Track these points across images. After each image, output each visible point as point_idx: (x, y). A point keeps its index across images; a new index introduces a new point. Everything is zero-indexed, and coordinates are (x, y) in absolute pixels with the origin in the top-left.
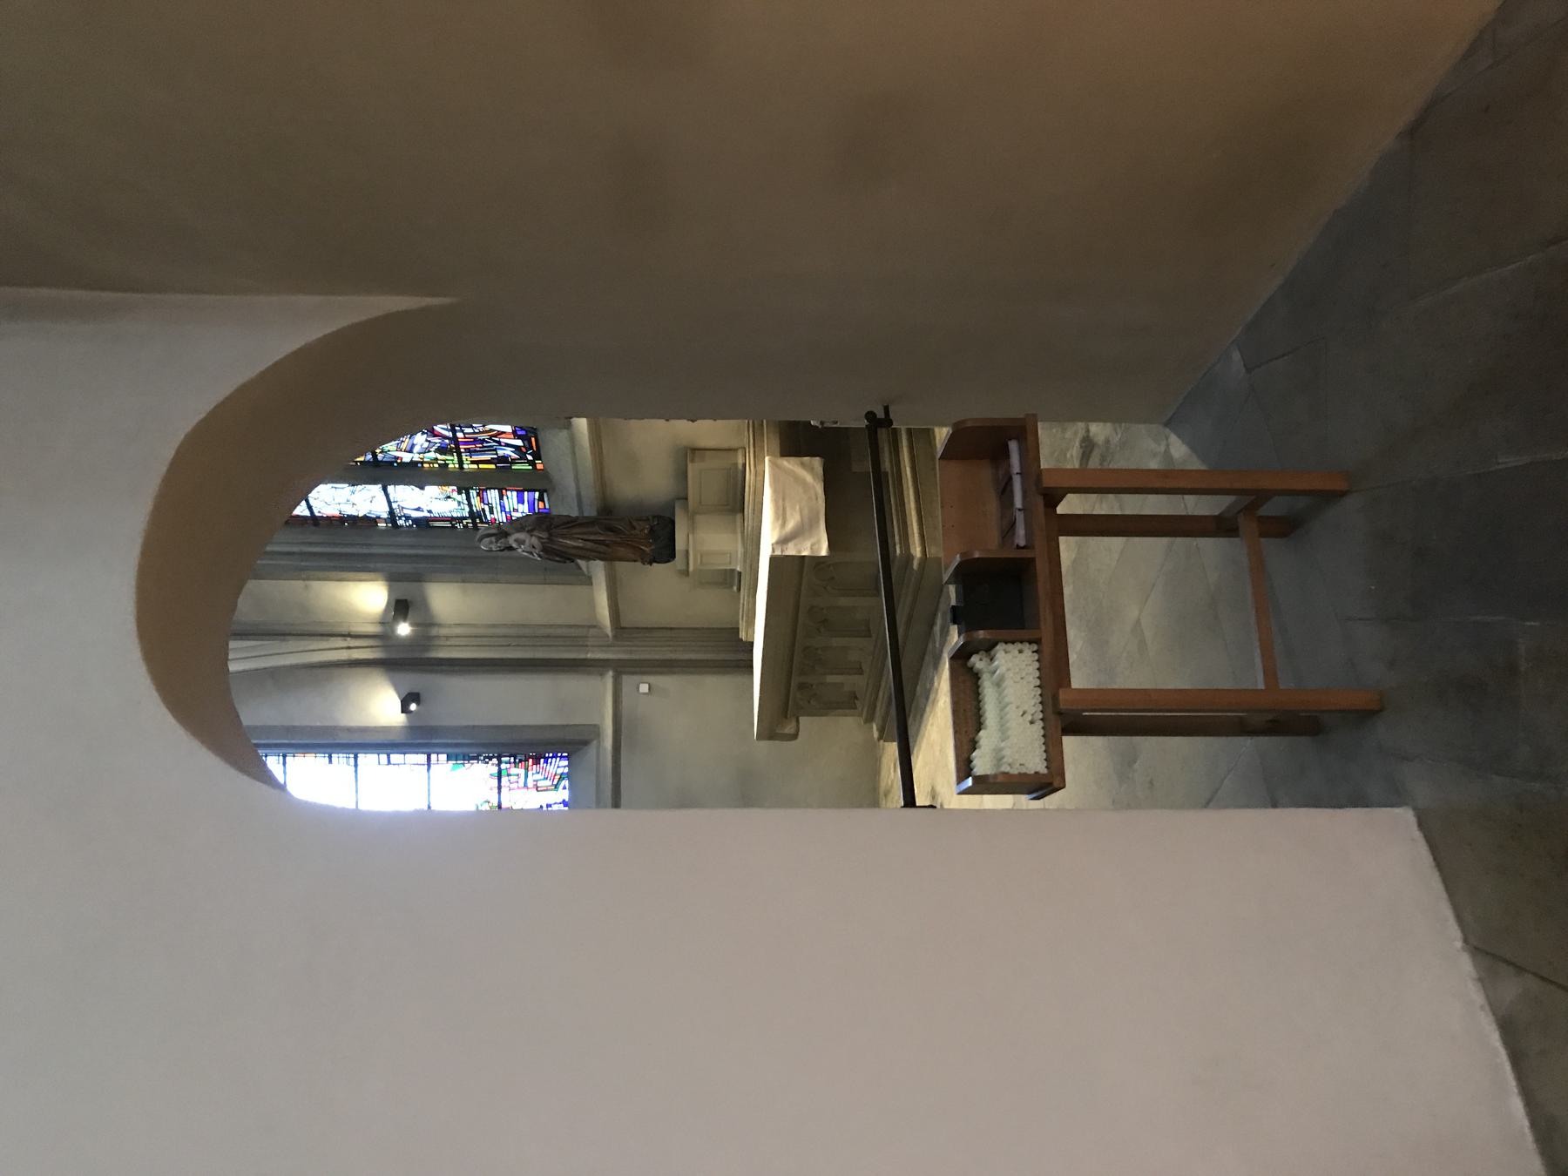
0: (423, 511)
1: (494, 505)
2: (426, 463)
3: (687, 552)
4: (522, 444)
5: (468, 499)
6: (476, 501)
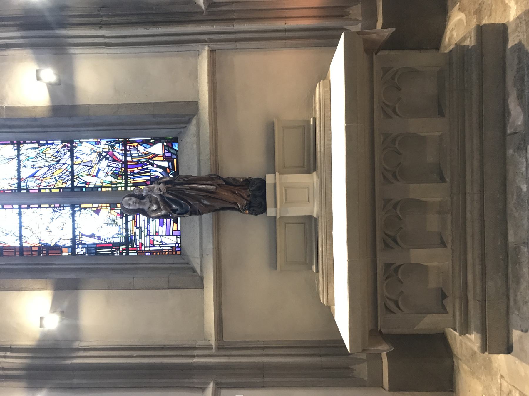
0: (94, 238)
1: (143, 229)
2: (104, 187)
3: (275, 185)
4: (167, 166)
5: (126, 223)
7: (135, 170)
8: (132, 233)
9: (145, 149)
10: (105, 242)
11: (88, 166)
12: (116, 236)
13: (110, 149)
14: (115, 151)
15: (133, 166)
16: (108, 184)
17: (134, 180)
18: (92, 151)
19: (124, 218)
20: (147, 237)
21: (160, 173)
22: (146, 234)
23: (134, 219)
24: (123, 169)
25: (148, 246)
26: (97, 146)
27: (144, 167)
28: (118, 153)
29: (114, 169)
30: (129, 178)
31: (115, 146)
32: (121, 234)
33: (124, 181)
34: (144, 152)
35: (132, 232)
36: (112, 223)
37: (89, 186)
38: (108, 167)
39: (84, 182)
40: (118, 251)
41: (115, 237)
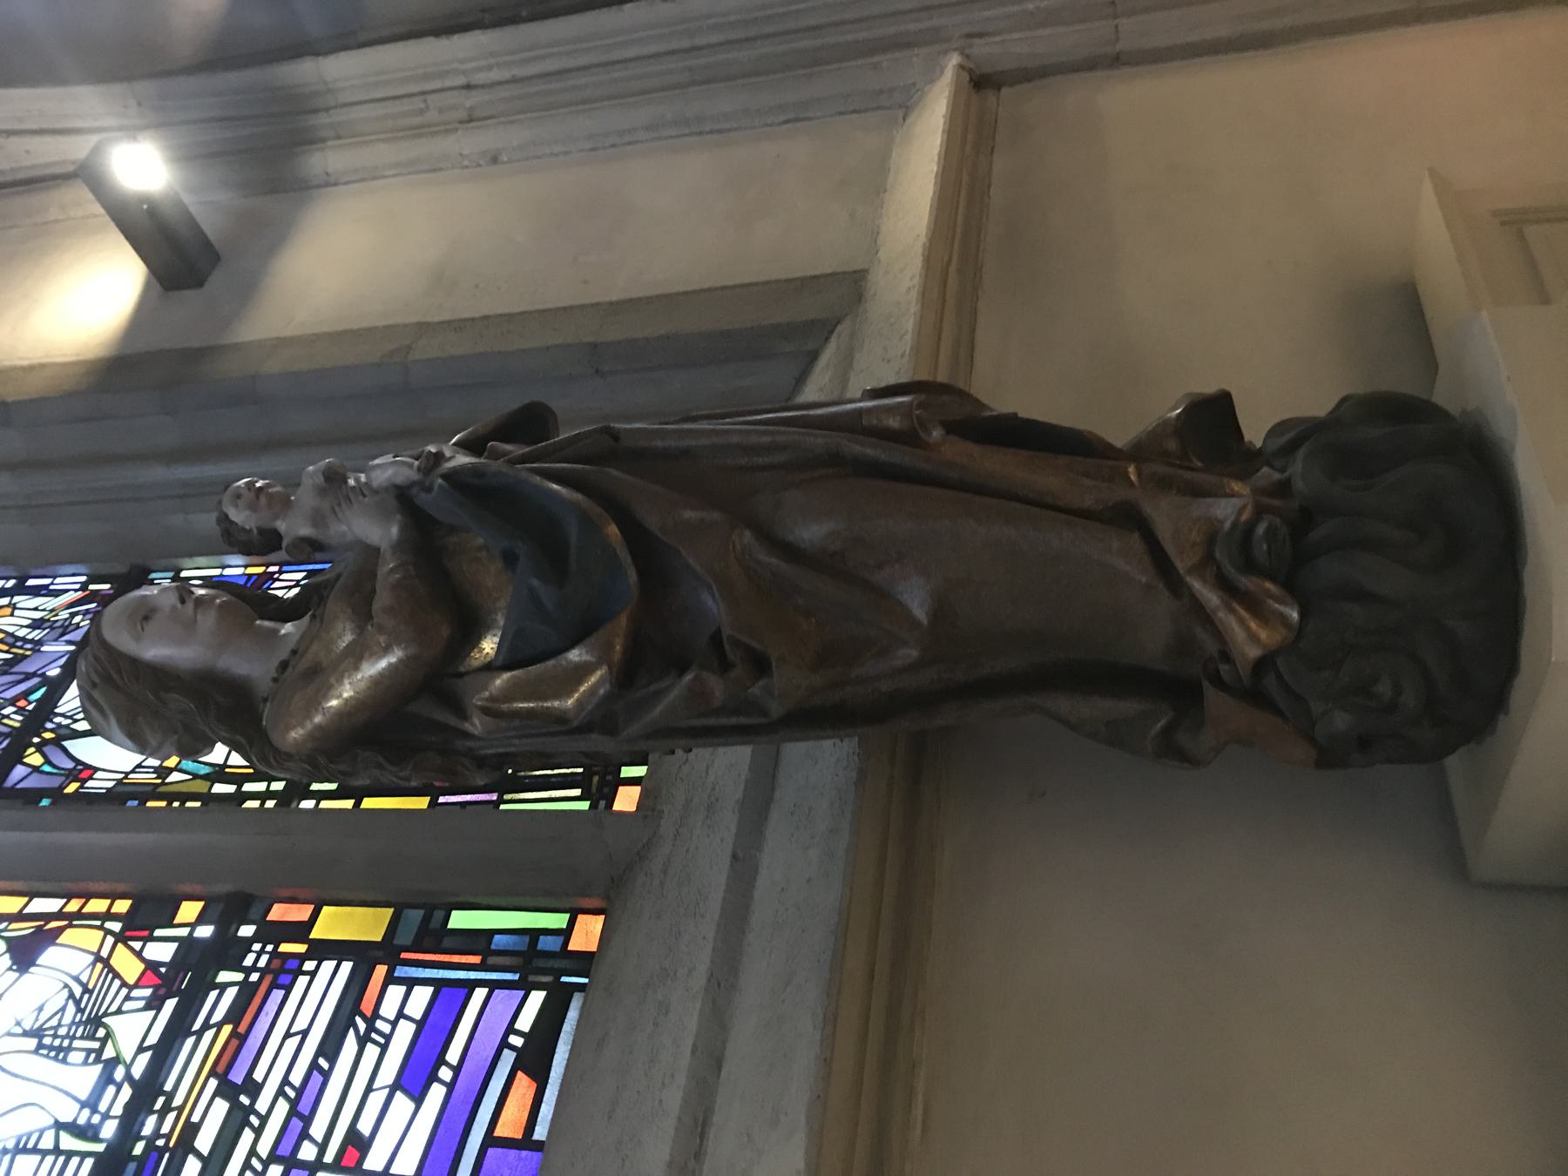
8: (165, 1129)
16: (196, 776)
22: (264, 1149)
23: (234, 1015)
35: (171, 1116)
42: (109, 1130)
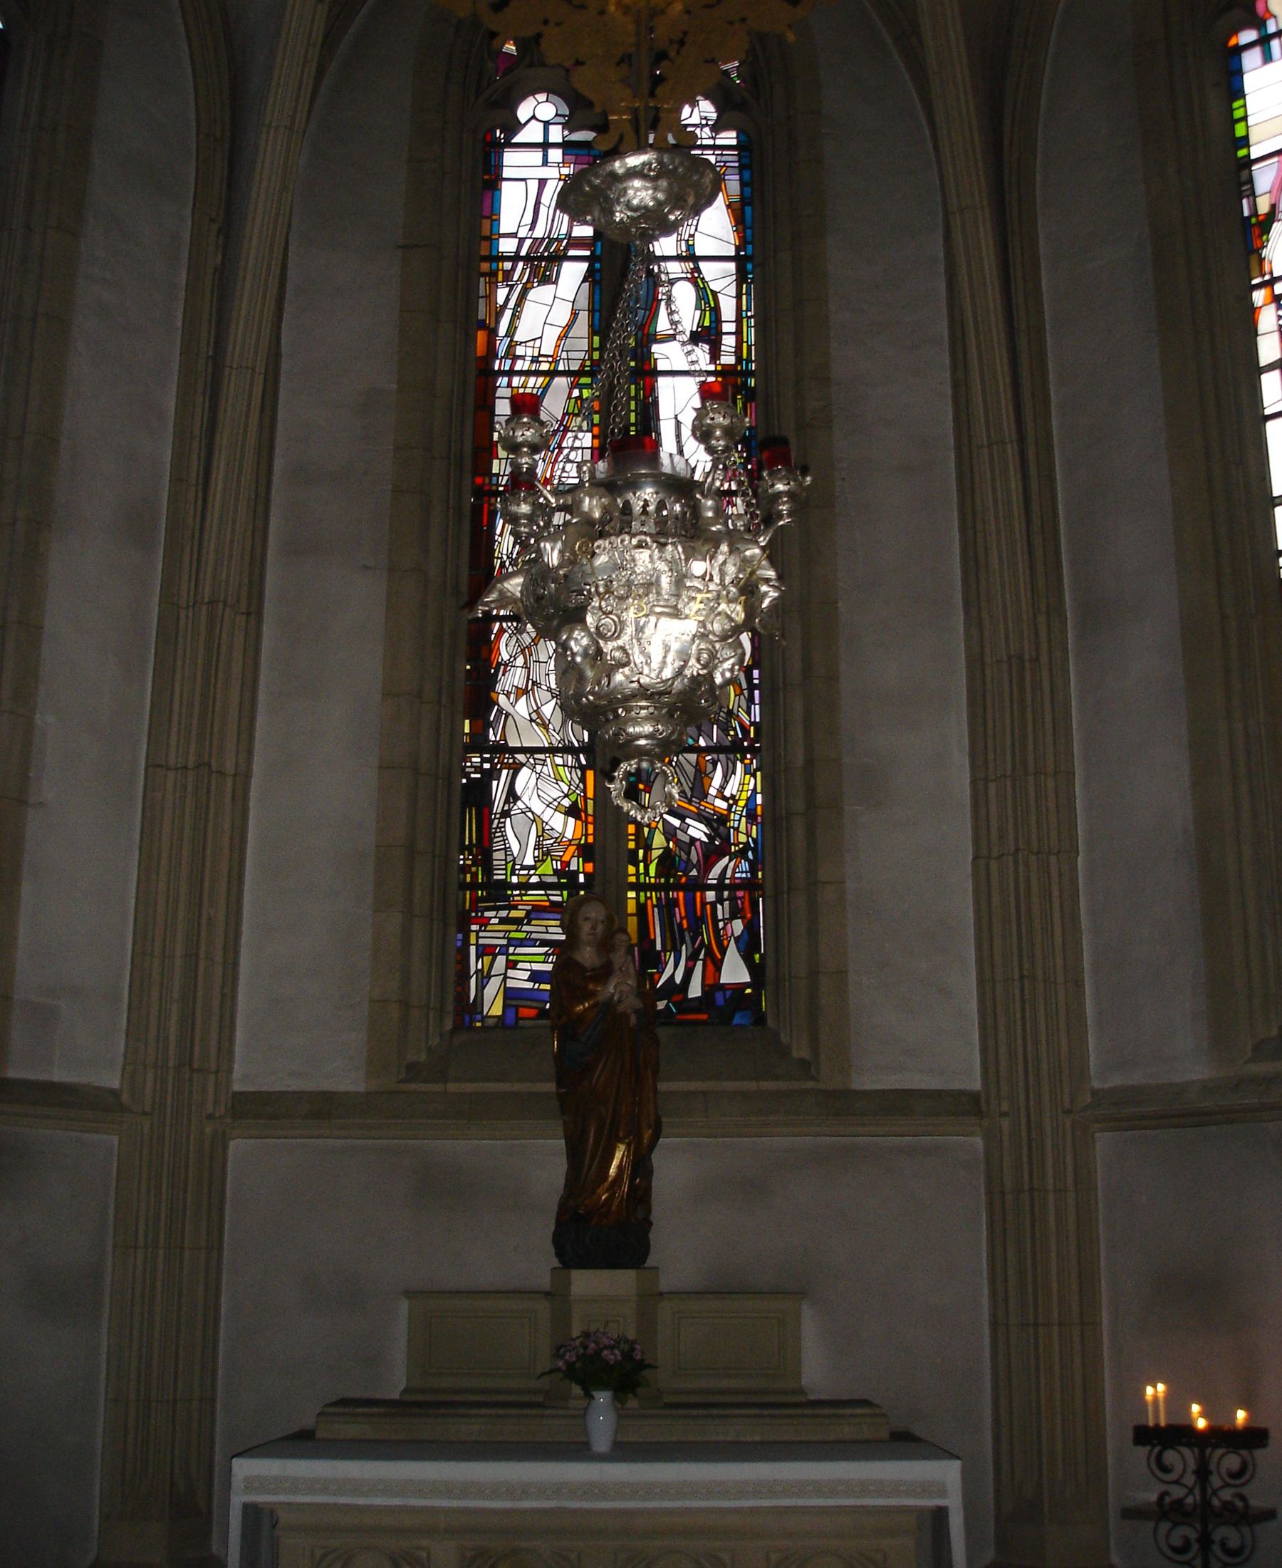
0: (507, 801)
1: (525, 928)
6: (536, 895)
7: (680, 912)
8: (516, 898)
9: (735, 938)
10: (496, 829)
11: (692, 789)
12: (509, 858)
13: (737, 848)
14: (730, 860)
15: (690, 903)
17: (653, 906)
18: (731, 802)
19: (554, 879)
20: (504, 938)
21: (673, 975)
22: (513, 935)
24: (684, 880)
25: (481, 941)
26: (744, 814)
27: (686, 933)
28: (727, 866)
29: (684, 856)
30: (658, 895)
31: (743, 861)
32: (513, 870)
33: (653, 880)
34: (726, 935)
35: (519, 898)
36: (543, 848)
37: (642, 790)
38: (688, 841)
39: (652, 780)
40: (469, 862)
41: (506, 855)
42: (515, 879)
